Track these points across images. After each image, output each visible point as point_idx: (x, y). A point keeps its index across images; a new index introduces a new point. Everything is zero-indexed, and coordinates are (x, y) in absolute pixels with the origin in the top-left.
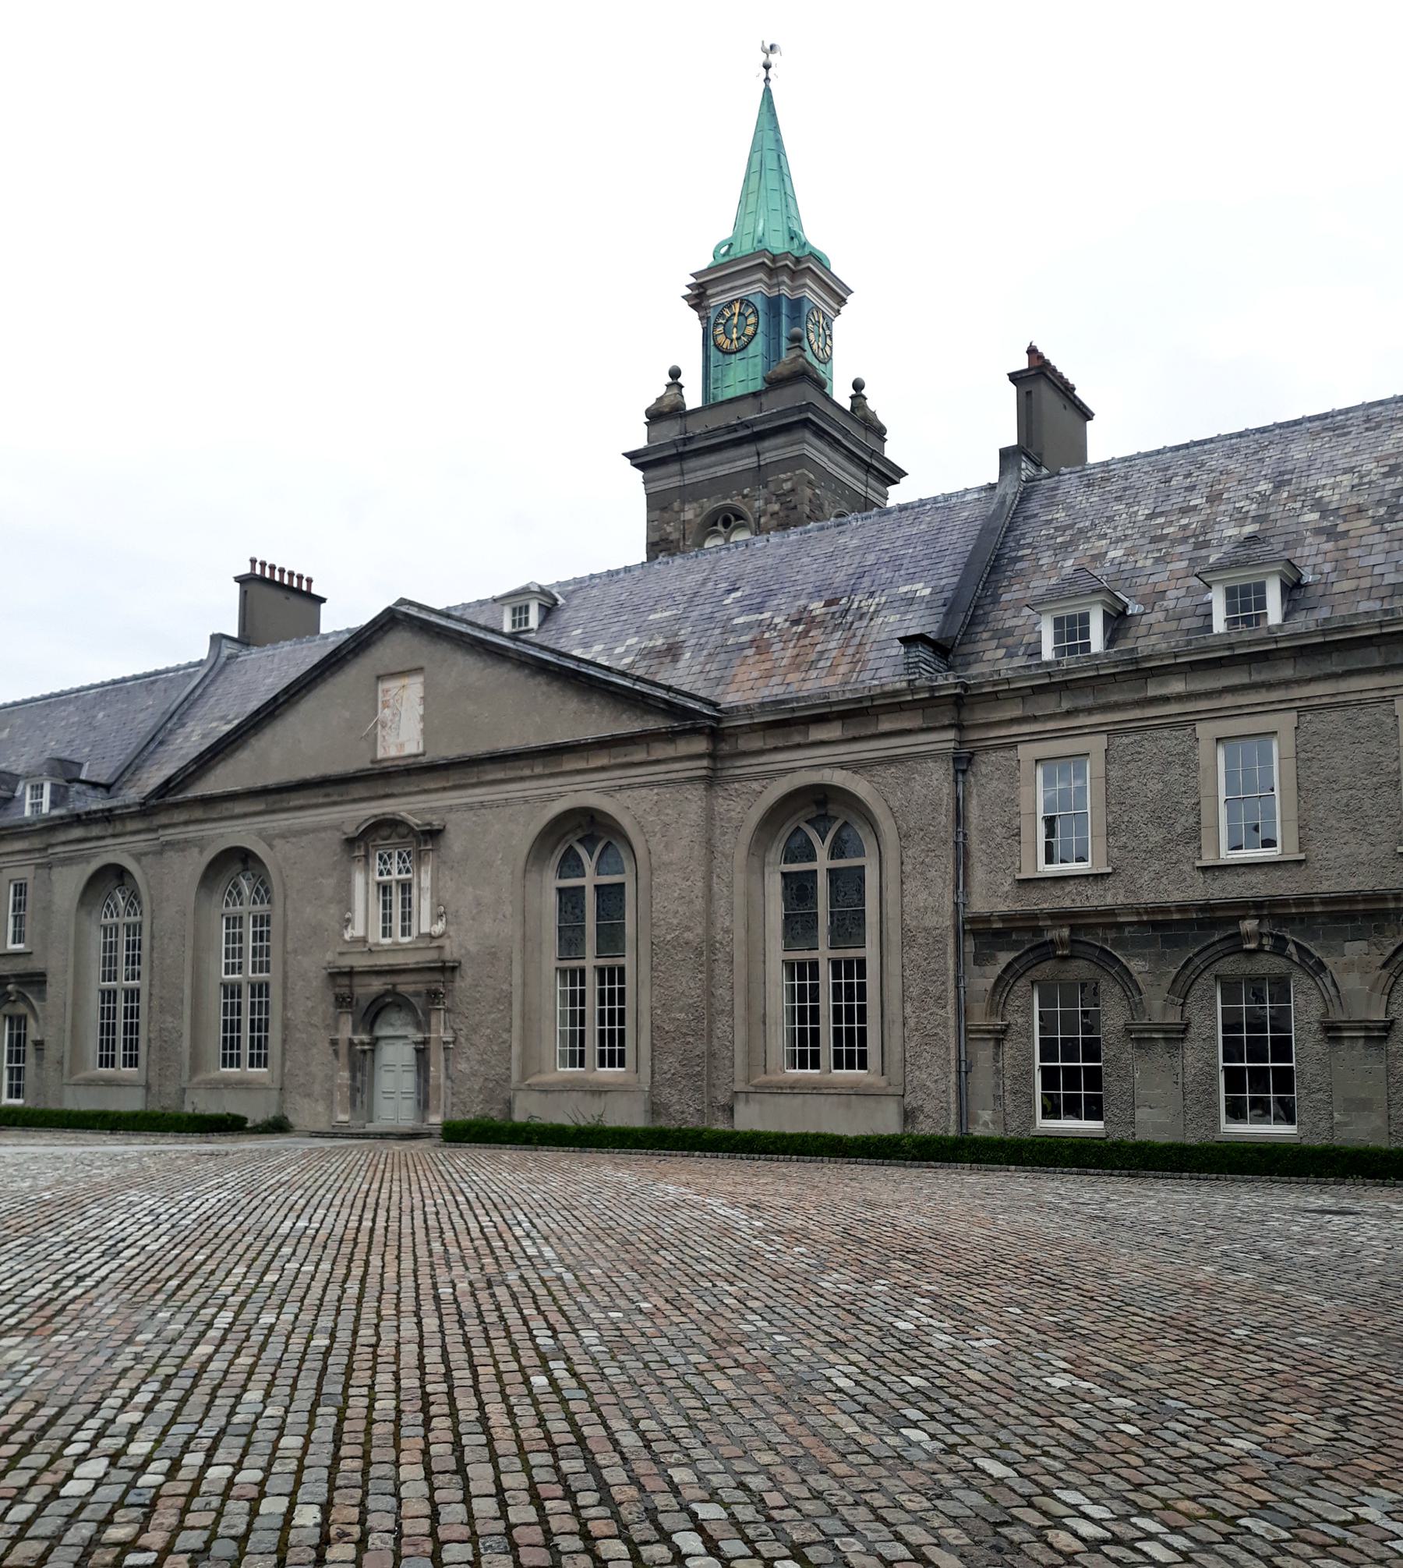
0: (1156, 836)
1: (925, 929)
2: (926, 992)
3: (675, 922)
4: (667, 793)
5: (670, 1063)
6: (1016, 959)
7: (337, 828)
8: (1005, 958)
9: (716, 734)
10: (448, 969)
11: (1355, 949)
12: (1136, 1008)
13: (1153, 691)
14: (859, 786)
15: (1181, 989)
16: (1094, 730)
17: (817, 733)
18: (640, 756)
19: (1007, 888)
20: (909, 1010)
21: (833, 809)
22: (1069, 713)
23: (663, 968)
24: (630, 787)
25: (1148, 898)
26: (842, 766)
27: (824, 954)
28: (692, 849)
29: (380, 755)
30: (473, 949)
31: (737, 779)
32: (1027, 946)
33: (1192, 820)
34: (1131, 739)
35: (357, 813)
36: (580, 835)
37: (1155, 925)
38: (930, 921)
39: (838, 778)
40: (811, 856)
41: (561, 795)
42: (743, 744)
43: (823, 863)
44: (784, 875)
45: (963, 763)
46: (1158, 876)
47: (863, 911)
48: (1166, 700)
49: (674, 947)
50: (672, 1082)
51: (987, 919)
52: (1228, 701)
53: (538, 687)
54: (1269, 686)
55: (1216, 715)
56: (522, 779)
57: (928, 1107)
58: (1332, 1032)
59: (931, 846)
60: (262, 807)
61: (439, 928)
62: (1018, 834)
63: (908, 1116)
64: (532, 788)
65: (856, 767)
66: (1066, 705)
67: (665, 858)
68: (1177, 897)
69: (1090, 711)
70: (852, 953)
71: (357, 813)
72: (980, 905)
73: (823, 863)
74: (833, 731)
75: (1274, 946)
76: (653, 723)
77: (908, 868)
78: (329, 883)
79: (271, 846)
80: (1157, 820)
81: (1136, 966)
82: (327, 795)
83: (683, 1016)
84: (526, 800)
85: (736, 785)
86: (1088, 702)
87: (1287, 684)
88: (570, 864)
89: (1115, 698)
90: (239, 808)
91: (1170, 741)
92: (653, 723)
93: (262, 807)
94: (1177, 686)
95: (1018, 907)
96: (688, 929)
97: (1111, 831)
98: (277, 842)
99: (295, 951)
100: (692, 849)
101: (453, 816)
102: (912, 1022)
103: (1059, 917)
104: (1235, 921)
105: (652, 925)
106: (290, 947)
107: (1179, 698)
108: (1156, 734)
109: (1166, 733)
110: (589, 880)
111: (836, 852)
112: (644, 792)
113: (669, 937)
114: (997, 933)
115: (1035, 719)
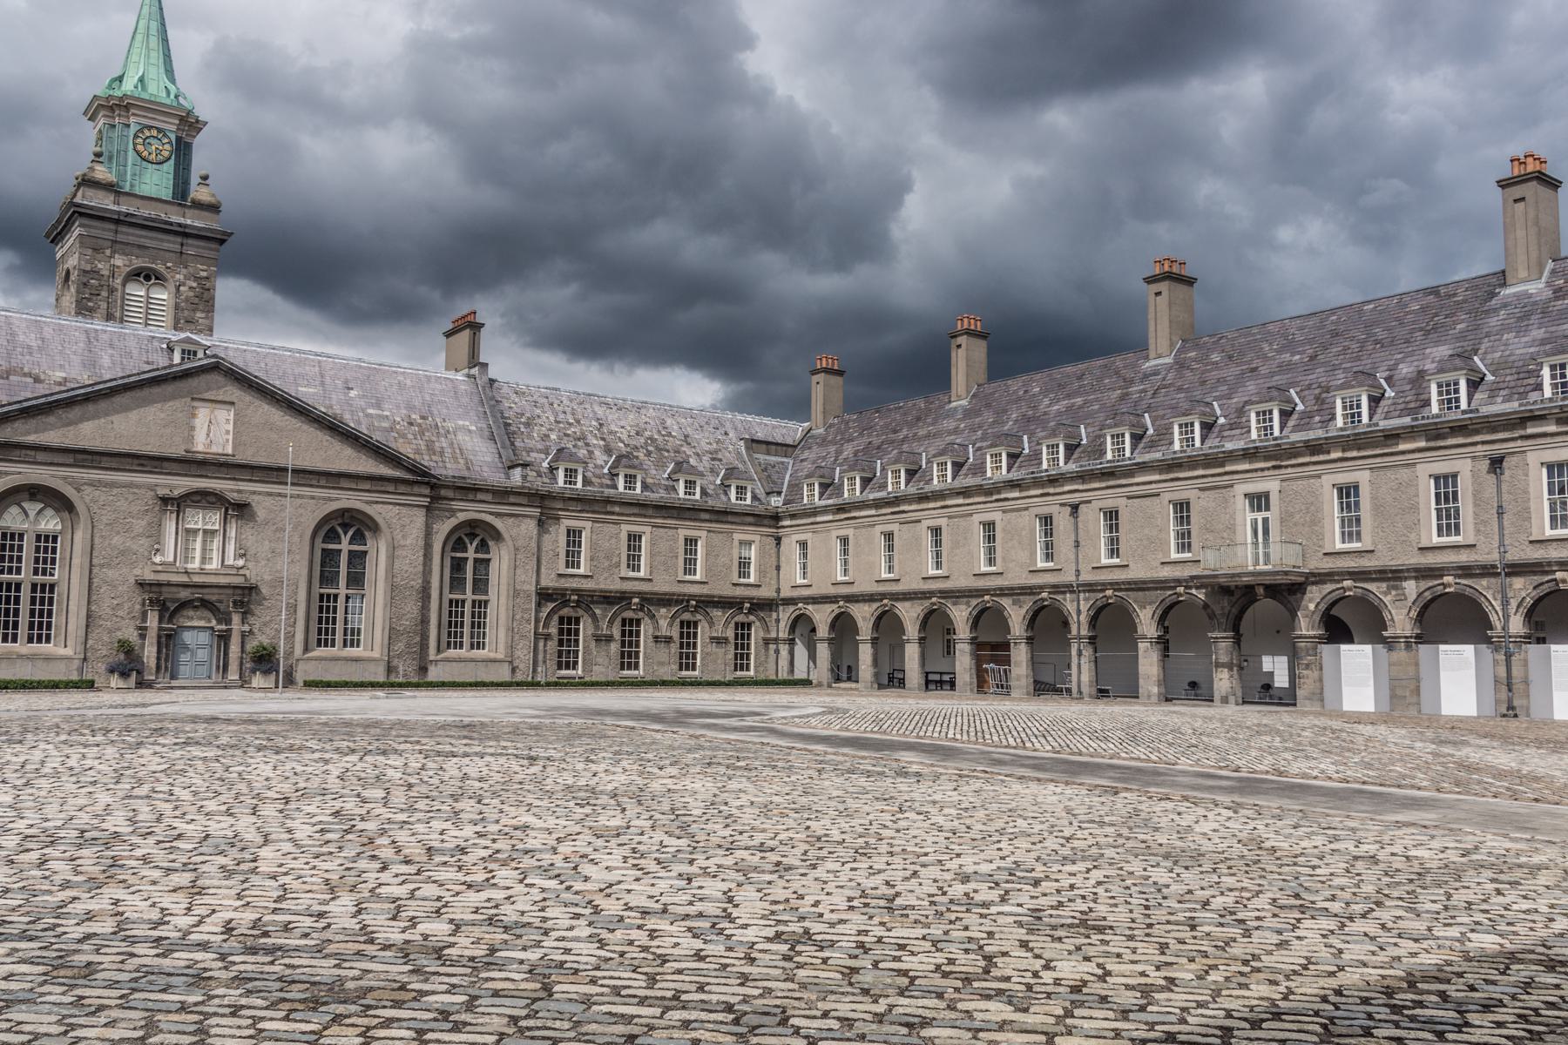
4: (404, 510)
5: (400, 646)
7: (152, 488)
8: (551, 606)
9: (433, 487)
10: (251, 589)
11: (663, 611)
12: (597, 627)
13: (609, 508)
14: (498, 523)
15: (611, 622)
16: (588, 519)
17: (480, 496)
18: (391, 489)
21: (478, 531)
22: (580, 511)
24: (377, 502)
25: (602, 586)
26: (491, 513)
27: (469, 596)
29: (200, 448)
30: (267, 577)
31: (439, 509)
35: (182, 484)
36: (340, 521)
37: (605, 597)
38: (526, 587)
40: (465, 550)
41: (337, 499)
42: (443, 492)
45: (541, 523)
48: (613, 513)
50: (399, 656)
51: (548, 589)
53: (324, 438)
54: (645, 516)
55: (629, 523)
56: (311, 486)
57: (522, 666)
58: (656, 639)
60: (71, 461)
61: (241, 562)
63: (514, 670)
64: (318, 492)
65: (498, 515)
67: (402, 543)
69: (588, 512)
70: (483, 598)
71: (182, 484)
72: (544, 583)
73: (471, 554)
74: (489, 497)
76: (397, 473)
78: (140, 525)
79: (79, 490)
80: (607, 558)
81: (598, 611)
82: (142, 465)
84: (313, 498)
86: (587, 508)
87: (651, 517)
88: (332, 536)
89: (597, 509)
90: (41, 456)
91: (612, 528)
92: (397, 473)
93: (71, 461)
94: (617, 509)
95: (557, 585)
98: (88, 489)
99: (102, 566)
101: (256, 498)
103: (575, 591)
104: (631, 598)
106: (95, 561)
107: (618, 514)
110: (345, 545)
114: (549, 595)
115: (568, 510)
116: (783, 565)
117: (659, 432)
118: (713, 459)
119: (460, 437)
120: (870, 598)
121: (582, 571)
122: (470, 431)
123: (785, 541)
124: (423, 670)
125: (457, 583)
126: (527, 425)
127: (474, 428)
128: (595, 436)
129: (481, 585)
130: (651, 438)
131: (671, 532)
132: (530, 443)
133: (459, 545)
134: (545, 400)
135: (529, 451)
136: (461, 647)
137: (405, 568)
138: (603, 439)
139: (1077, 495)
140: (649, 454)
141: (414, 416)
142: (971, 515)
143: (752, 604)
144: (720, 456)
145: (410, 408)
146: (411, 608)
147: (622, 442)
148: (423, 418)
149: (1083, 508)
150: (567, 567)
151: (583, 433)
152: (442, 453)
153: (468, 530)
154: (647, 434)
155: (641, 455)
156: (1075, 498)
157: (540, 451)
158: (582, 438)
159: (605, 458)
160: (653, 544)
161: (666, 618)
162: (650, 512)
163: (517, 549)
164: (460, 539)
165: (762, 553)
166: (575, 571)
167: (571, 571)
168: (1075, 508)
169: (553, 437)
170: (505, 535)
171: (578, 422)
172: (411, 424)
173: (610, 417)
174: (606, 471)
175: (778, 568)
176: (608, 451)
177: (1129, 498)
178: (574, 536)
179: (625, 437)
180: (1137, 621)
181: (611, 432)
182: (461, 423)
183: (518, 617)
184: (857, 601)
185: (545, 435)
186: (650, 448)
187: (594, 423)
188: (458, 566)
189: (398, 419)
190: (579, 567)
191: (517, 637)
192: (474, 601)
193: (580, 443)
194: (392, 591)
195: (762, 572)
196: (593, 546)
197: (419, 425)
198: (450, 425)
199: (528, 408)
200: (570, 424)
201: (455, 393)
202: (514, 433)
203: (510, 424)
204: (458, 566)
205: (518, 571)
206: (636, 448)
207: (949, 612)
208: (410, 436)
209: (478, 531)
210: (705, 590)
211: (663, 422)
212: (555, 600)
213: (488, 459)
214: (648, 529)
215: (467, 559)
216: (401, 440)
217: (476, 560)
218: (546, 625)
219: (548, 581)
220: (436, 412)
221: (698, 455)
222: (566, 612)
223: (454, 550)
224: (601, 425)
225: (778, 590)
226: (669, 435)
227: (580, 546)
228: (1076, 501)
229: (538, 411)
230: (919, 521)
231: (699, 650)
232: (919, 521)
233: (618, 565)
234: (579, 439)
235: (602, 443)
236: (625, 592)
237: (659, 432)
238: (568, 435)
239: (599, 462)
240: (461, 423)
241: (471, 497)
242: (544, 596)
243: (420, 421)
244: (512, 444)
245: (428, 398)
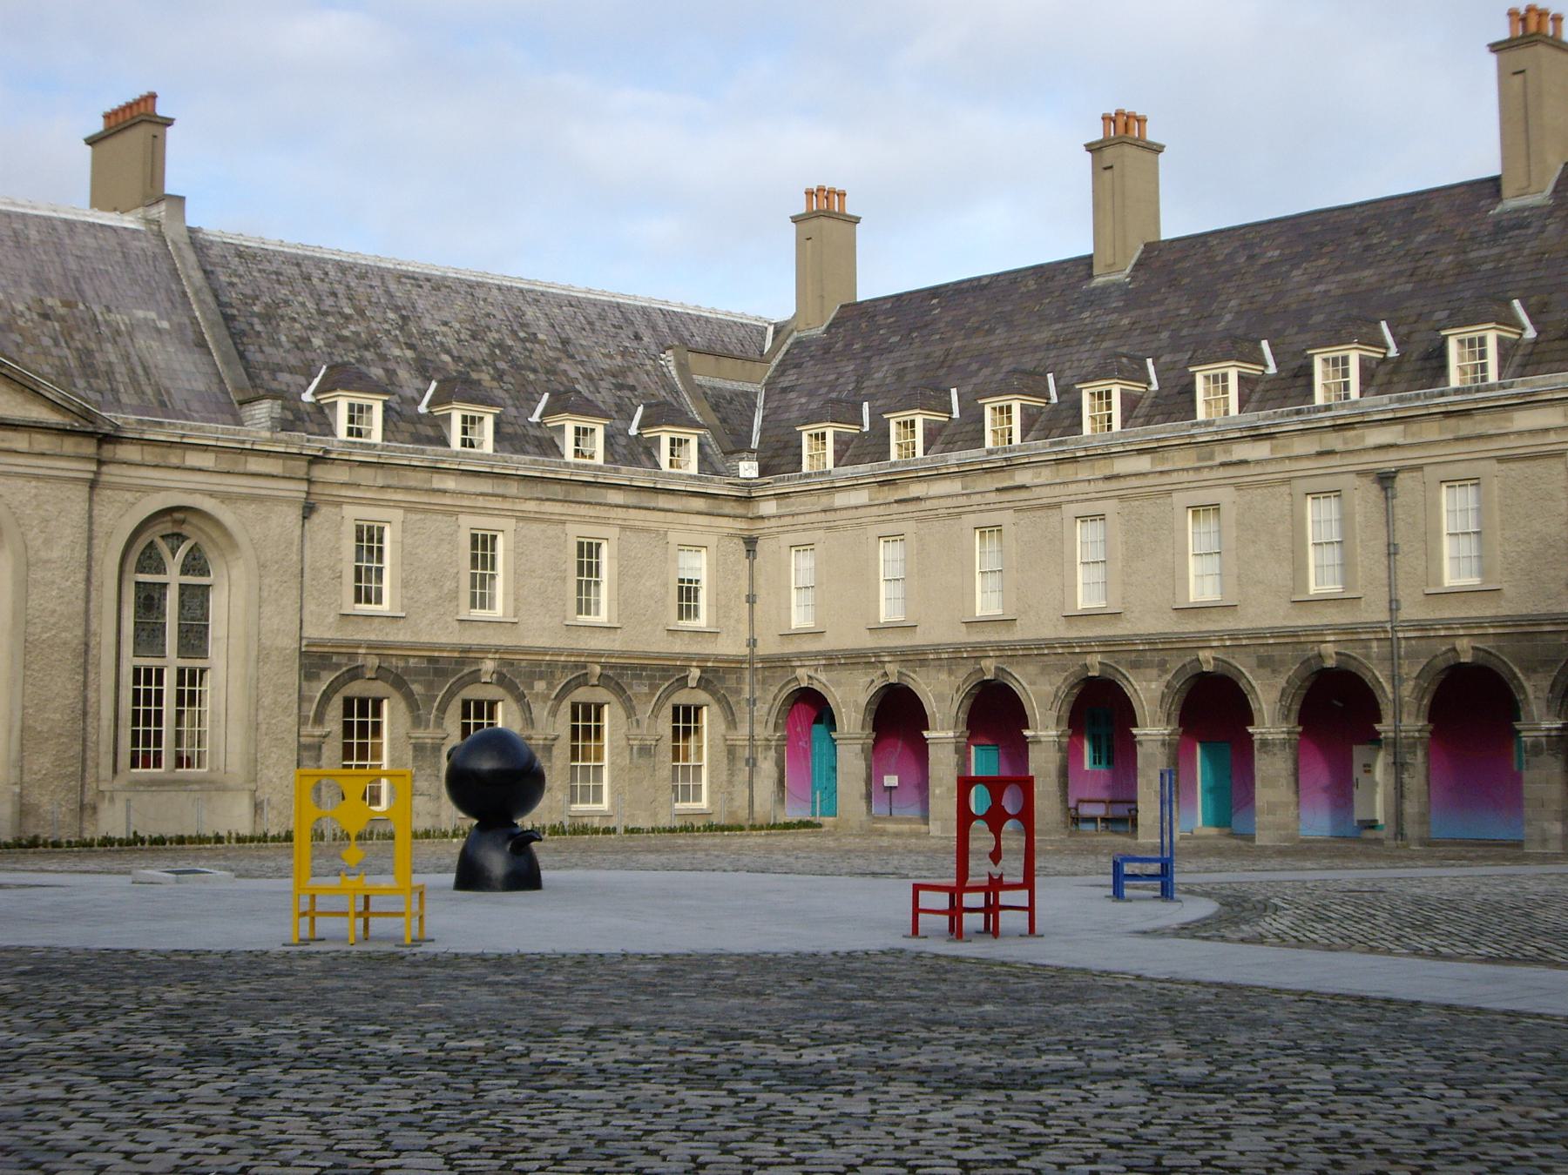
0: (433, 594)
1: (277, 649)
2: (275, 702)
3: (52, 620)
4: (47, 489)
5: (42, 762)
6: (337, 678)
8: (328, 678)
16: (396, 504)
17: (193, 459)
19: (331, 619)
20: (261, 717)
23: (36, 667)
26: (211, 494)
28: (72, 550)
32: (344, 669)
33: (454, 585)
34: (419, 516)
39: (207, 504)
40: (160, 568)
43: (173, 577)
44: (137, 583)
46: (432, 624)
47: (207, 627)
49: (50, 647)
52: (480, 502)
57: (275, 799)
59: (285, 578)
62: (340, 577)
63: (257, 807)
65: (226, 497)
66: (380, 482)
67: (43, 554)
68: (443, 640)
70: (198, 663)
72: (311, 632)
73: (173, 577)
75: (498, 680)
77: (265, 594)
81: (417, 688)
83: (58, 716)
85: (109, 492)
91: (440, 523)
95: (338, 636)
96: (66, 629)
97: (405, 584)
100: (72, 550)
102: (263, 727)
105: (27, 622)
108: (434, 517)
109: (440, 517)
111: (185, 571)
112: (20, 482)
113: (45, 636)
116: (762, 594)
117: (514, 333)
118: (620, 387)
119: (141, 342)
120: (953, 656)
121: (385, 607)
122: (159, 331)
123: (762, 546)
124: (86, 809)
125: (149, 634)
126: (267, 318)
127: (165, 325)
128: (396, 340)
129: (194, 637)
130: (500, 345)
131: (552, 530)
132: (277, 355)
133: (151, 560)
134: (295, 271)
135: (275, 369)
136: (158, 764)
137: (51, 606)
138: (411, 347)
139: (1393, 454)
140: (499, 376)
141: (49, 301)
142: (1169, 492)
143: (704, 670)
144: (631, 381)
145: (41, 284)
146: (63, 686)
147: (449, 352)
148: (67, 304)
149: (1403, 481)
150: (358, 600)
151: (373, 336)
152: (110, 375)
153: (166, 527)
154: (493, 336)
155: (485, 377)
156: (1388, 461)
157: (292, 370)
158: (373, 344)
159: (418, 383)
160: (518, 552)
161: (546, 697)
162: (513, 488)
163: (262, 566)
164: (151, 545)
165: (719, 568)
166: (371, 608)
167: (364, 608)
168: (1386, 480)
169: (317, 342)
170: (241, 537)
171: (361, 313)
172: (45, 316)
173: (421, 304)
174: (422, 409)
175: (751, 599)
176: (424, 369)
177: (1500, 460)
178: (368, 541)
179: (451, 342)
180: (1520, 697)
181: (425, 334)
182: (140, 314)
183: (267, 701)
184: (923, 663)
185: (302, 339)
186: (502, 365)
187: (391, 315)
188: (149, 600)
189: (20, 307)
190: (379, 601)
191: (265, 743)
192: (181, 672)
193: (369, 355)
194: (27, 652)
195: (719, 608)
196: (407, 557)
197: (62, 319)
198: (118, 318)
199: (264, 284)
200: (347, 318)
201: (125, 255)
202: (243, 333)
203: (233, 318)
204: (149, 600)
205: (268, 610)
206: (473, 364)
207: (1123, 683)
208: (47, 342)
209: (186, 530)
210: (614, 643)
211: (520, 315)
212: (338, 666)
213: (200, 386)
214: (509, 524)
215: (165, 585)
216: (29, 350)
217: (183, 588)
218: (319, 719)
219: (322, 629)
220: (90, 294)
221: (591, 379)
222: (356, 689)
223: (141, 569)
224: (403, 317)
225: (752, 643)
226: (533, 338)
227: (380, 560)
228: (1389, 466)
229: (284, 292)
230: (1058, 505)
231: (606, 762)
232: (1058, 505)
233: (454, 596)
234: (366, 347)
235: (409, 354)
236: (469, 650)
237: (514, 333)
238: (341, 339)
239: (409, 392)
240: (140, 314)
241: (174, 460)
242: (313, 660)
243: (62, 311)
244: (242, 355)
245: (73, 265)
